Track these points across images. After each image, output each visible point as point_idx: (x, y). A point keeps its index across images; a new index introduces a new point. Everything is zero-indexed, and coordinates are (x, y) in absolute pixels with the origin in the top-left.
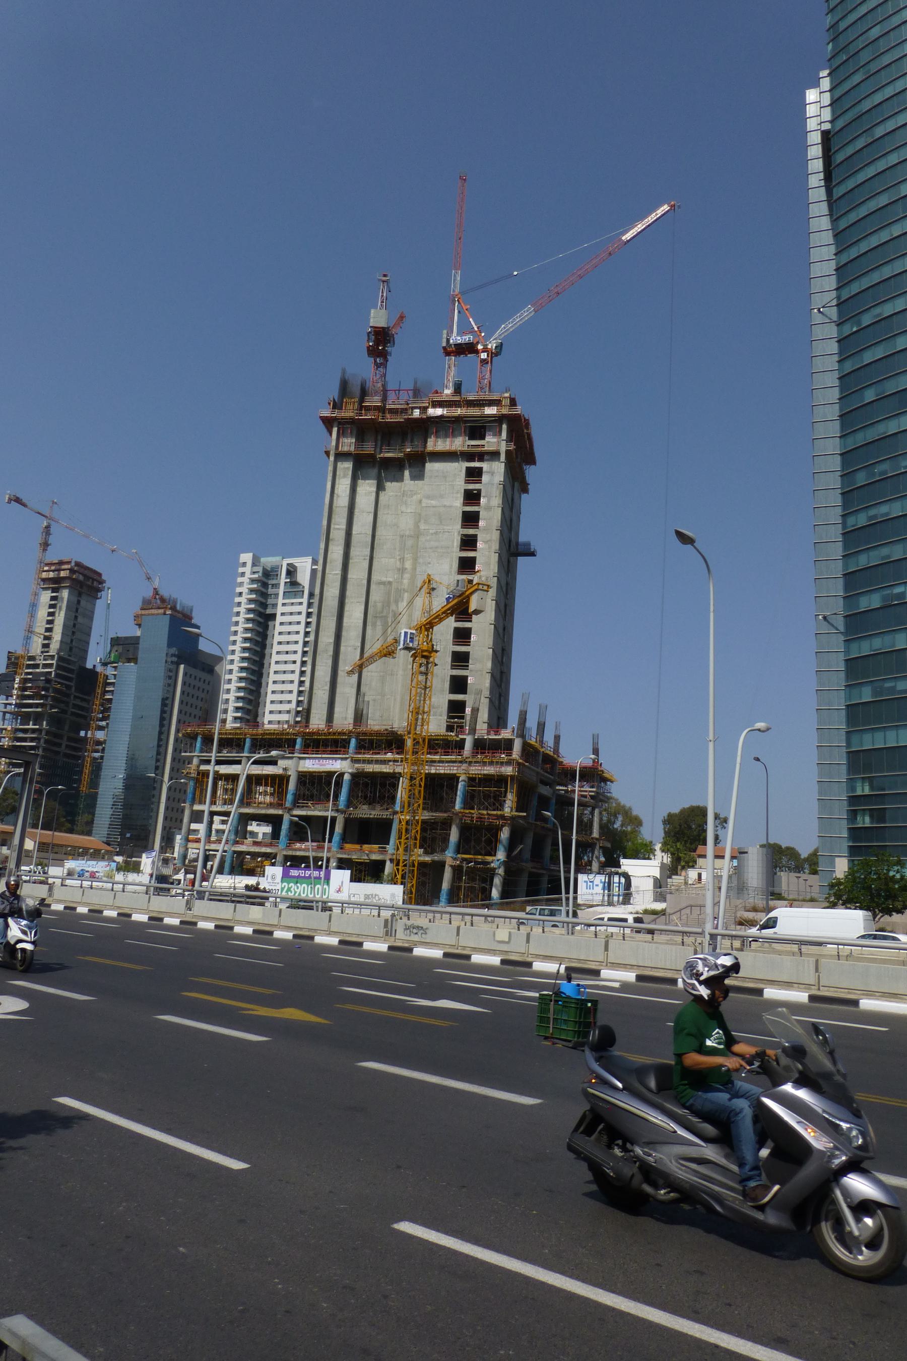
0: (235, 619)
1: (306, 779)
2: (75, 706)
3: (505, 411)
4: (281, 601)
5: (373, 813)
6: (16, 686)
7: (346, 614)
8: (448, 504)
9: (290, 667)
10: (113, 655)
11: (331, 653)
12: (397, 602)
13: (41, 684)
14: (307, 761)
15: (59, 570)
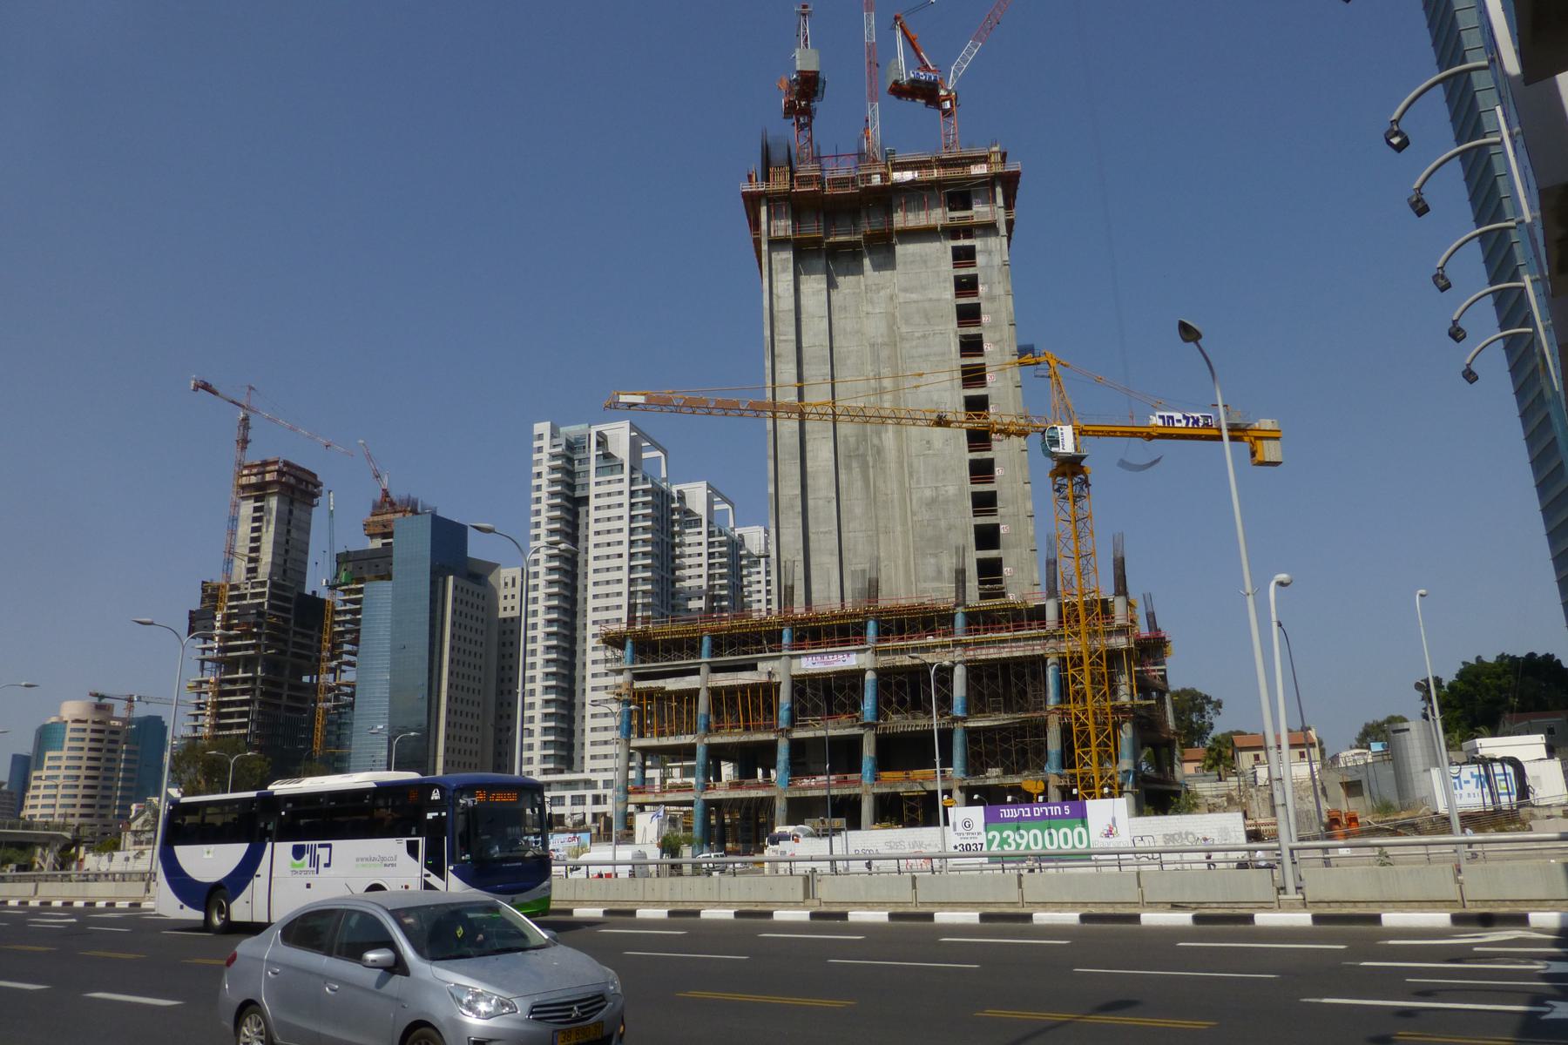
0: (534, 507)
1: (801, 684)
2: (295, 643)
3: (998, 169)
4: (593, 479)
5: (919, 722)
6: (218, 624)
7: (809, 455)
8: (934, 297)
9: (615, 562)
10: (343, 575)
11: (799, 509)
12: (879, 434)
13: (252, 619)
14: (804, 660)
15: (263, 473)
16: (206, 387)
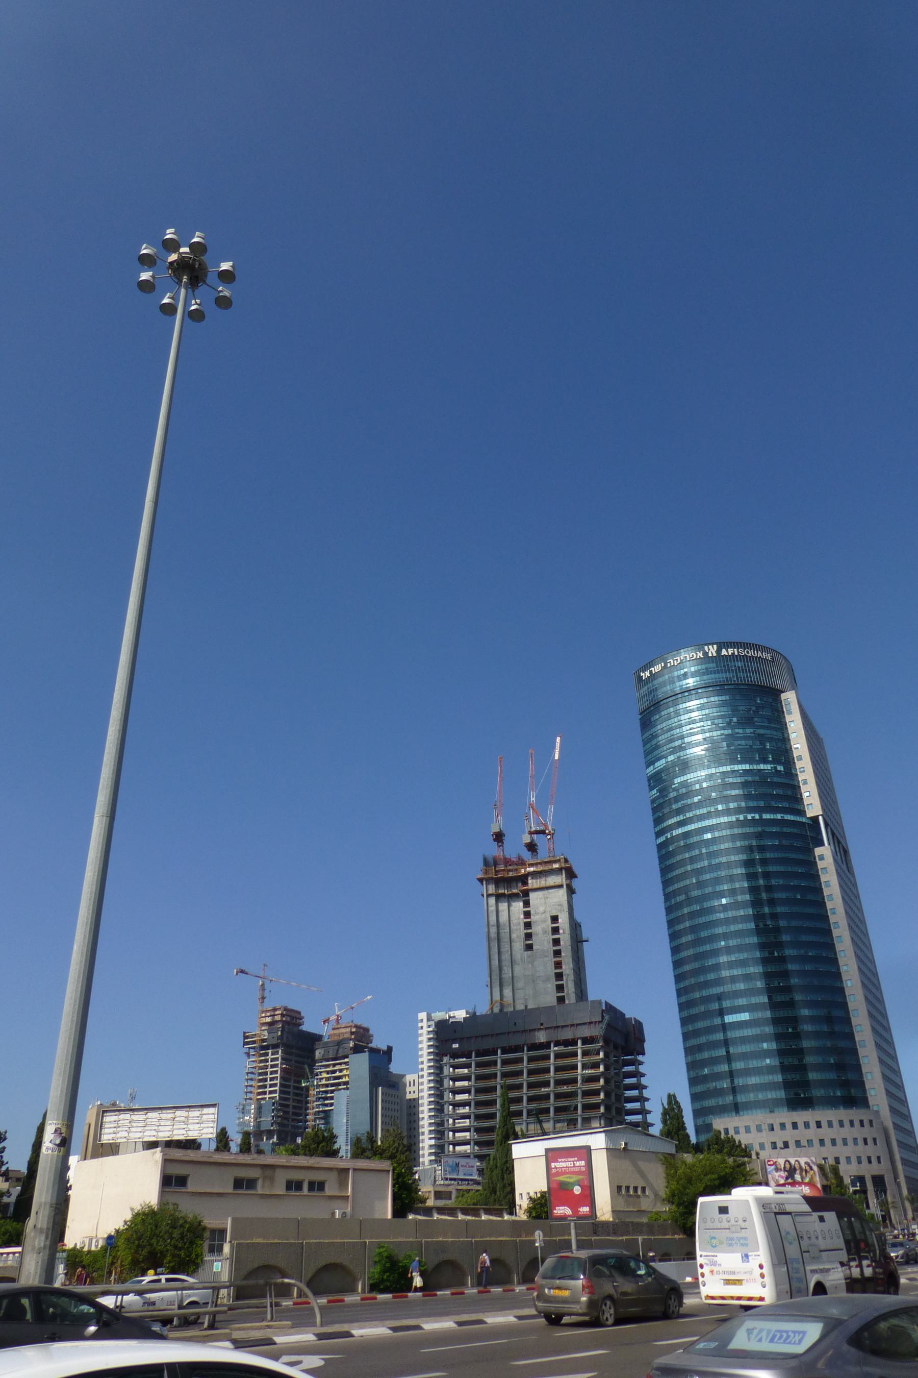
3: (563, 865)
16: (242, 972)
